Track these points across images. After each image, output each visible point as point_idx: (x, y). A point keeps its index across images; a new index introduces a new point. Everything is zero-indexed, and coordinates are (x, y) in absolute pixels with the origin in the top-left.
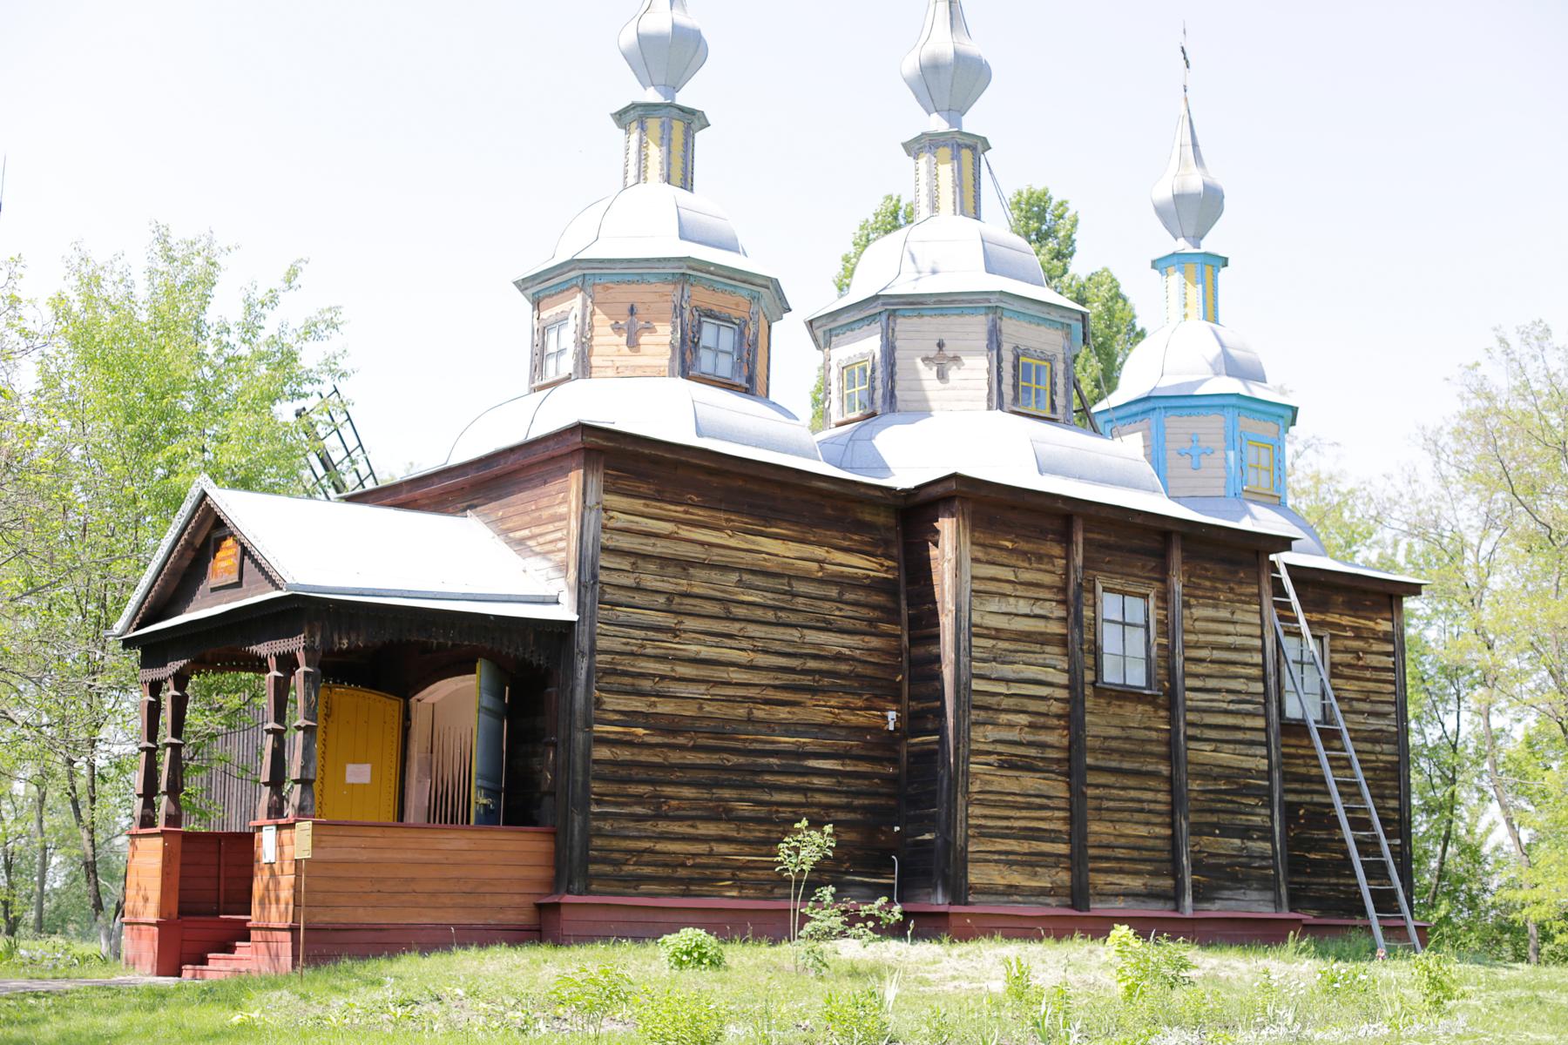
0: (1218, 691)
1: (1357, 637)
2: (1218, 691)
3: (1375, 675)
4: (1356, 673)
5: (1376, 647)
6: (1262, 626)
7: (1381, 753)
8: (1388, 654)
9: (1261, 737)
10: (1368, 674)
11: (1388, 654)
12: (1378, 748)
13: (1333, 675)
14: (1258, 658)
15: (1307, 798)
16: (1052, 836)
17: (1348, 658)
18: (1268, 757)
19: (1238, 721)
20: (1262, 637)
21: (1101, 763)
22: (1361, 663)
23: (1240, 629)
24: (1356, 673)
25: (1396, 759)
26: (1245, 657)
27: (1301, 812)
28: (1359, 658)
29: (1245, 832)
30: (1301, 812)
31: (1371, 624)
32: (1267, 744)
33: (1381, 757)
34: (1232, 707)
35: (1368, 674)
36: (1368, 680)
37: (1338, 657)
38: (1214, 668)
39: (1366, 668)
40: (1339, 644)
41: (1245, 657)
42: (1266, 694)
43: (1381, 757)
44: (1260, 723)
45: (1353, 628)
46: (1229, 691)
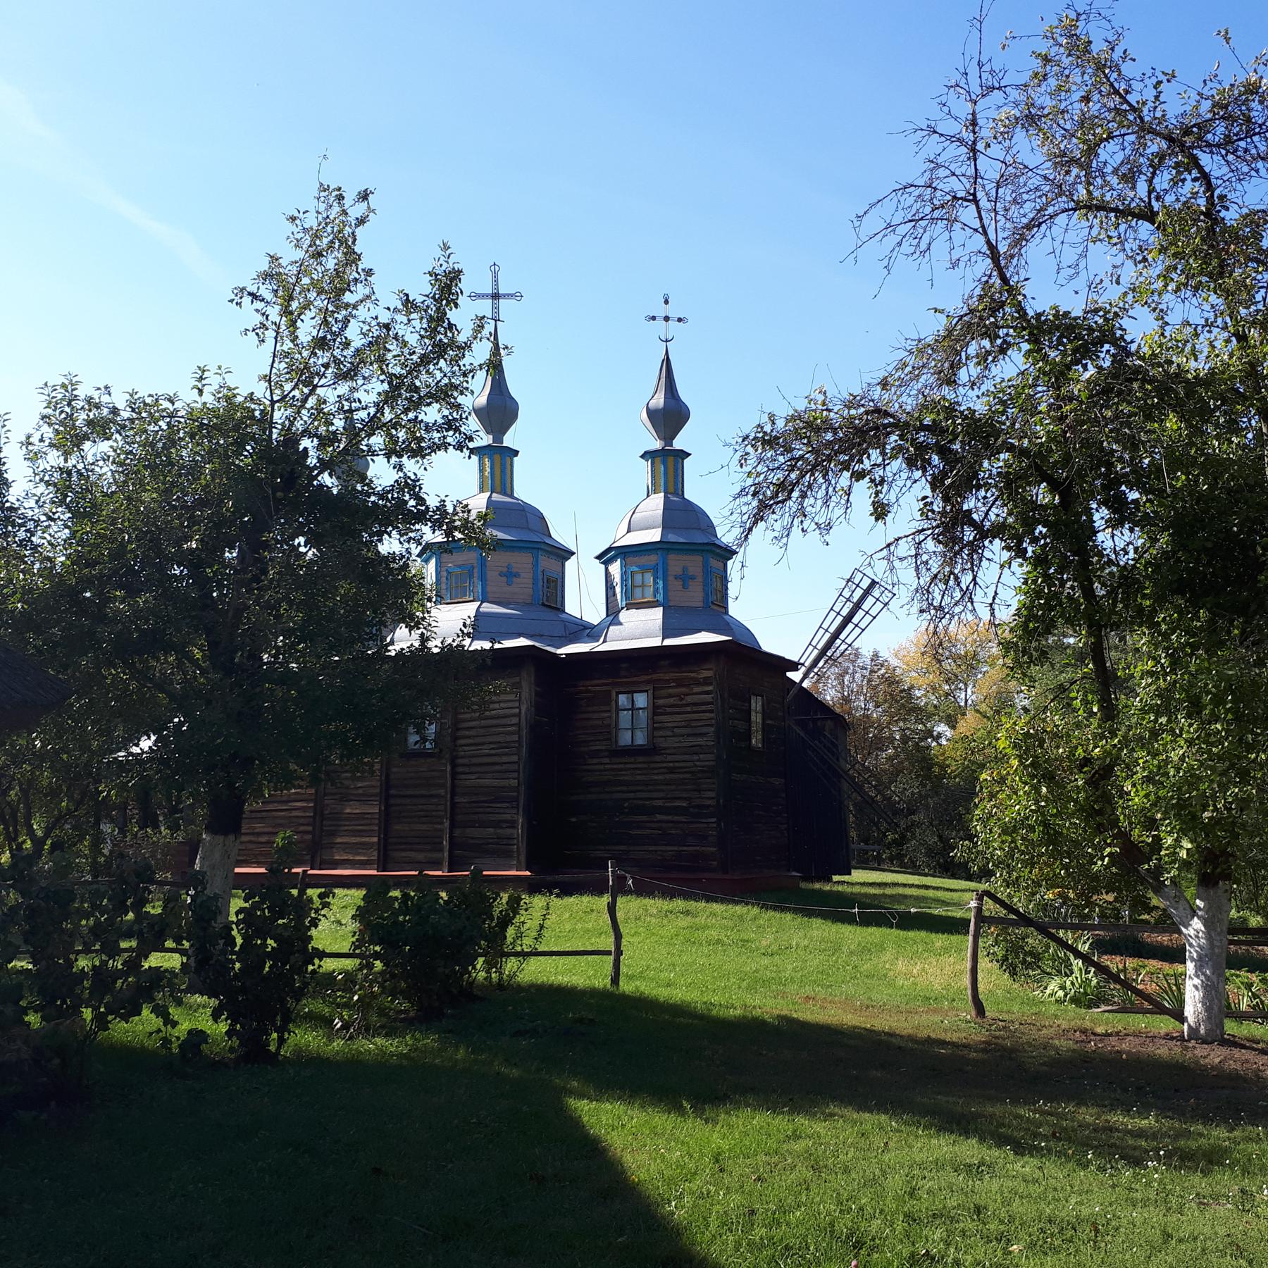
0: (483, 744)
1: (678, 686)
2: (483, 744)
3: (695, 709)
4: (677, 710)
5: (696, 690)
6: (520, 701)
7: (698, 761)
8: (708, 693)
9: (516, 767)
10: (689, 709)
11: (708, 693)
12: (696, 757)
13: (655, 714)
14: (515, 720)
15: (632, 795)
16: (369, 833)
17: (672, 700)
18: (518, 779)
19: (496, 759)
20: (519, 708)
21: (402, 793)
22: (684, 702)
23: (502, 705)
24: (677, 710)
25: (713, 763)
26: (507, 721)
27: (626, 805)
28: (682, 699)
29: (497, 824)
30: (626, 805)
31: (692, 675)
32: (518, 771)
33: (698, 763)
34: (493, 752)
35: (689, 709)
36: (689, 713)
37: (661, 702)
38: (482, 731)
39: (687, 705)
40: (663, 692)
41: (507, 721)
42: (519, 742)
43: (698, 763)
44: (515, 758)
45: (674, 680)
46: (491, 743)
